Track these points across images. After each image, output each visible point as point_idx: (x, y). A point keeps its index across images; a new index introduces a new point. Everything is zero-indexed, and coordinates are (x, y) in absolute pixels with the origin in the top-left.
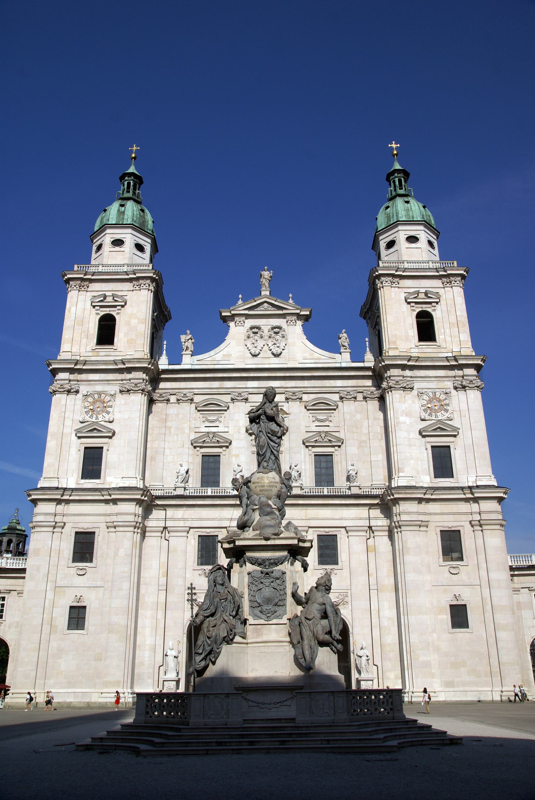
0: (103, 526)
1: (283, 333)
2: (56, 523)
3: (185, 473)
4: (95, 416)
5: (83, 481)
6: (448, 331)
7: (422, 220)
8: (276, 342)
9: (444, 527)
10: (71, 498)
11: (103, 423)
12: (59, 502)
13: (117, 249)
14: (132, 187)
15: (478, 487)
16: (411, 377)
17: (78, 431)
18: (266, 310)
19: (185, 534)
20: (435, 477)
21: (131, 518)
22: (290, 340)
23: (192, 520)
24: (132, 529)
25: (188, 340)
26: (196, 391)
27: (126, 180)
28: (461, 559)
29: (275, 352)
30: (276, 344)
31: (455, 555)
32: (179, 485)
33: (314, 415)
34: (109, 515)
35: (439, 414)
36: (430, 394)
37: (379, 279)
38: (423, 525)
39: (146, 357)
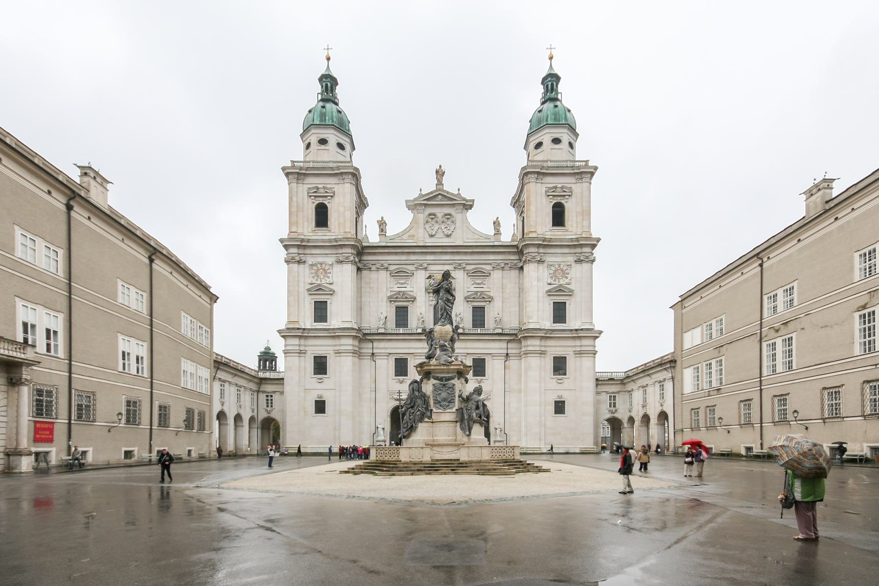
0: (332, 352)
1: (452, 219)
2: (300, 350)
3: (385, 319)
4: (319, 280)
5: (316, 324)
6: (575, 218)
7: (566, 123)
8: (447, 226)
9: (556, 355)
10: (309, 335)
11: (325, 285)
12: (300, 337)
13: (323, 147)
14: (329, 89)
15: (582, 329)
16: (544, 253)
17: (309, 290)
18: (441, 200)
19: (386, 357)
20: (554, 323)
21: (350, 348)
22: (458, 225)
23: (391, 348)
24: (351, 354)
25: (383, 223)
26: (390, 262)
27: (324, 82)
28: (565, 374)
29: (446, 233)
30: (446, 227)
31: (561, 372)
32: (381, 326)
33: (474, 280)
34: (335, 345)
35: (561, 280)
36: (557, 266)
37: (526, 176)
38: (542, 353)
39: (353, 237)
